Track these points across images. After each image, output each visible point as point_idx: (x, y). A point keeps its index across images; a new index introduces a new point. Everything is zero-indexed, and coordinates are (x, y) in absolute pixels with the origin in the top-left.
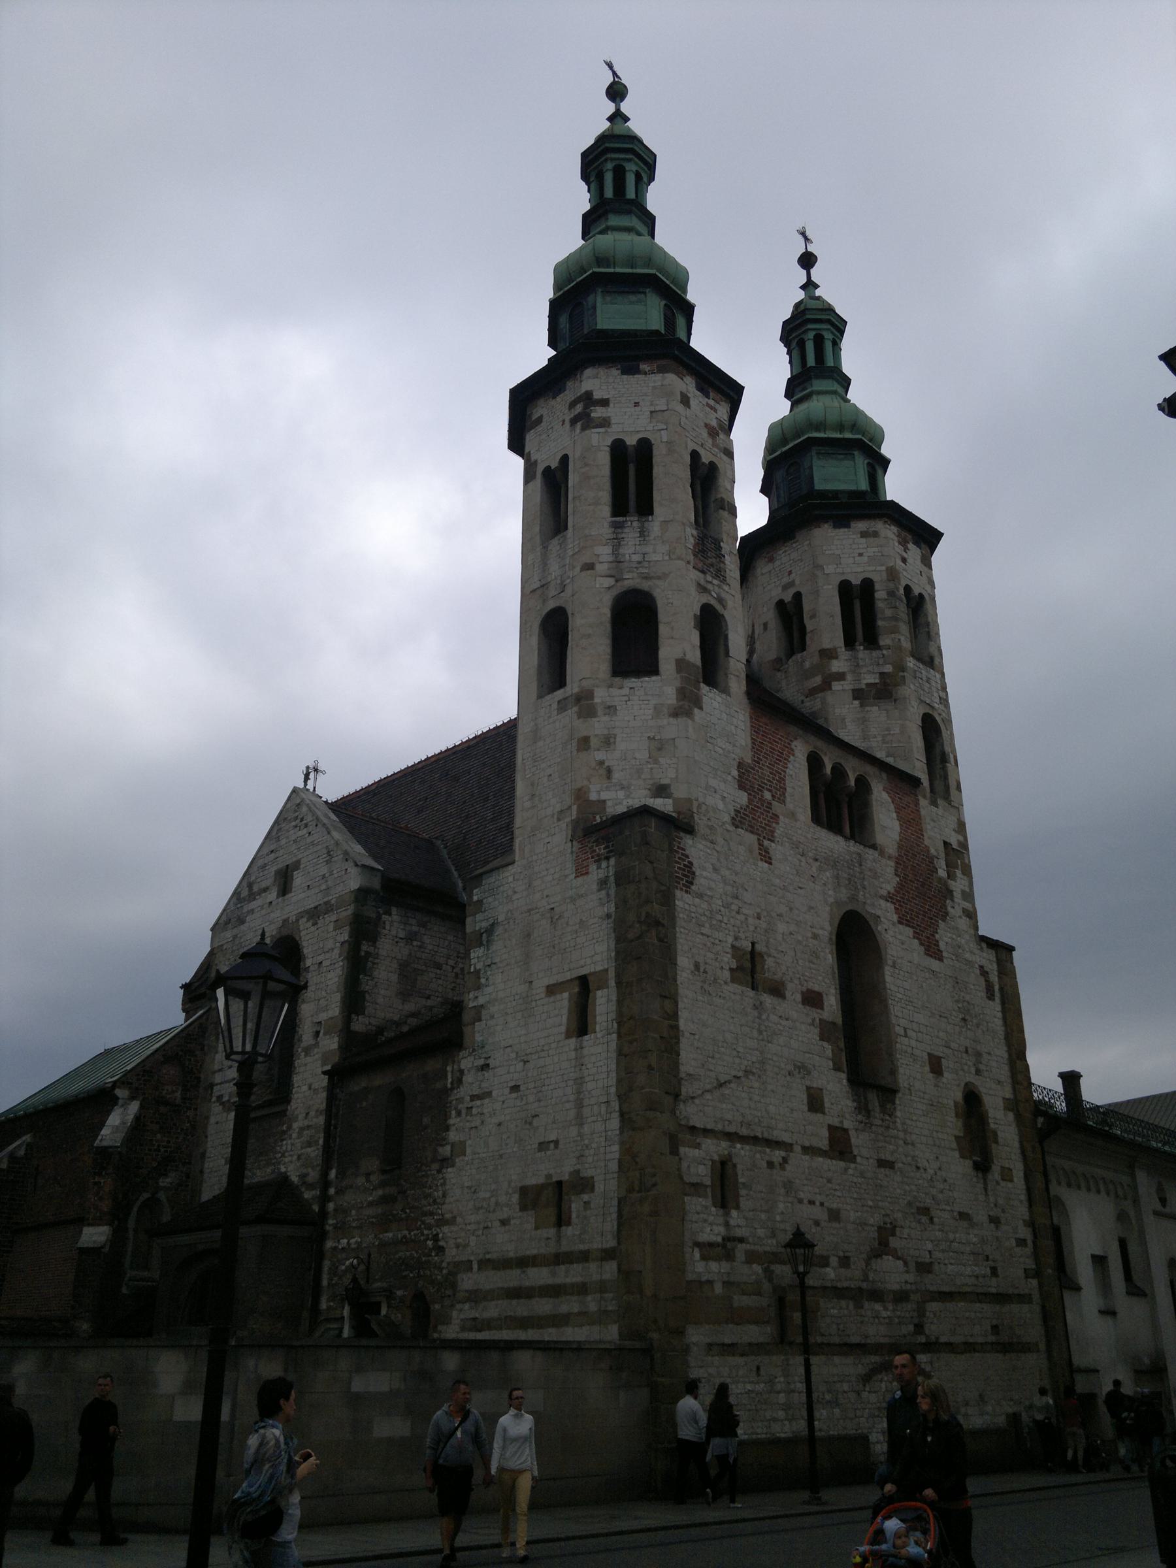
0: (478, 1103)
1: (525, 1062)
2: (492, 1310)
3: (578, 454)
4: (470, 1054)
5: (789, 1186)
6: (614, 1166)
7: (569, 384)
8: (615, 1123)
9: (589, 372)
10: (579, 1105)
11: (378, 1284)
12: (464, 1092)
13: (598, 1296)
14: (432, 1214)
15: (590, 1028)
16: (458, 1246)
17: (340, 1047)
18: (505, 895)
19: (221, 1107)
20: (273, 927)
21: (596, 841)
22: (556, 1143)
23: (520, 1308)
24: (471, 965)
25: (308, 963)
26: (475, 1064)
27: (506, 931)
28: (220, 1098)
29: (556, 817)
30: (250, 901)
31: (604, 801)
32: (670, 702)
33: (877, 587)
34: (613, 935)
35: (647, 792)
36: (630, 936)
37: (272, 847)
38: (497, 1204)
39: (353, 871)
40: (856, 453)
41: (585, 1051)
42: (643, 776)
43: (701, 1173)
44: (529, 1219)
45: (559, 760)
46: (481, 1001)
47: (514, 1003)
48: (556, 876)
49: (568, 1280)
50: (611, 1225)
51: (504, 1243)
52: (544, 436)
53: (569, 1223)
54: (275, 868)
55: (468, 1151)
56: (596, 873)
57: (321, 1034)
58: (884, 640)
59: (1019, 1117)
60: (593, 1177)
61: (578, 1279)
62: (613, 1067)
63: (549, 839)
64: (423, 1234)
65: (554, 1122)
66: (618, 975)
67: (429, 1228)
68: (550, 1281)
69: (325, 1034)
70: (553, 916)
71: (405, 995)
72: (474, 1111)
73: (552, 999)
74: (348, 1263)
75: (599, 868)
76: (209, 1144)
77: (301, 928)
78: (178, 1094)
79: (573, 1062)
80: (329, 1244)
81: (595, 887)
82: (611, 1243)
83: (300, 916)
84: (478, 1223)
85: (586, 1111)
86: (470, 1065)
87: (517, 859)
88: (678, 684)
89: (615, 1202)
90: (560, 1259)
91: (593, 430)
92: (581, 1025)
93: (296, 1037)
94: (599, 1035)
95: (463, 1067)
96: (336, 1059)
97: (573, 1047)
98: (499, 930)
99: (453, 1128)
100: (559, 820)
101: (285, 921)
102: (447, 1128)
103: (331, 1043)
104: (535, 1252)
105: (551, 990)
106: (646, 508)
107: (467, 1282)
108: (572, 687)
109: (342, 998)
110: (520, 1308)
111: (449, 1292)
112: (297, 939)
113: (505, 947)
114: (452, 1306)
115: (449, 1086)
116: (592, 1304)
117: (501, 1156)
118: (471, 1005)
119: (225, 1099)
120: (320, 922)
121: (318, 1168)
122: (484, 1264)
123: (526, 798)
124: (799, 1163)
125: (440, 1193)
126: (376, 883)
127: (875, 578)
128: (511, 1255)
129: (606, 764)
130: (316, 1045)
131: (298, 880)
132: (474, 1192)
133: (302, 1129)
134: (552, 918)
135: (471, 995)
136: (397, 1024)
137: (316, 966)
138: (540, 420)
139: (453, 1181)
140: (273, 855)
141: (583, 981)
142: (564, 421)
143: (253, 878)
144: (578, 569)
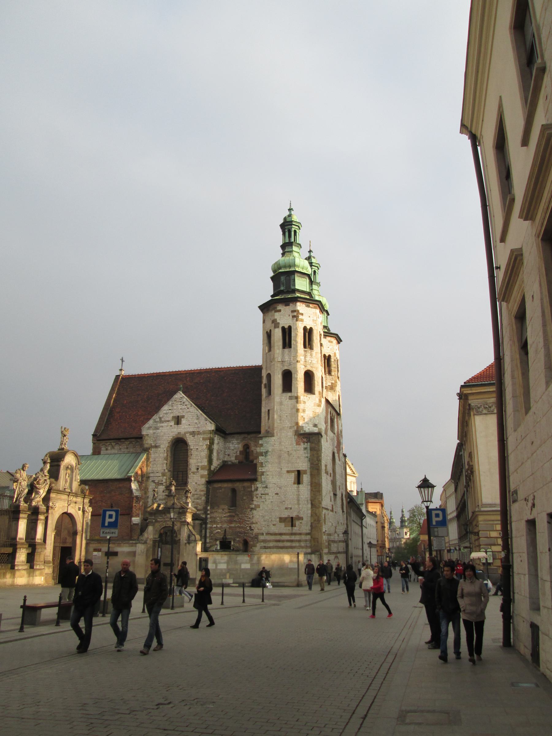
0: (264, 496)
1: (280, 488)
2: (271, 544)
3: (295, 328)
4: (260, 483)
5: (329, 518)
6: (309, 515)
7: (291, 304)
8: (310, 506)
9: (298, 304)
10: (298, 500)
11: (229, 537)
12: (258, 492)
13: (305, 543)
14: (249, 521)
15: (301, 482)
16: (258, 529)
17: (208, 474)
18: (271, 444)
19: (154, 484)
20: (173, 433)
21: (304, 438)
22: (291, 508)
23: (280, 544)
24: (259, 461)
25: (192, 448)
26: (263, 486)
27: (272, 454)
28: (153, 481)
29: (289, 428)
30: (160, 423)
31: (303, 427)
32: (317, 402)
33: (332, 358)
34: (309, 462)
35: (312, 426)
36: (315, 463)
37: (170, 408)
38: (271, 520)
39: (209, 424)
40: (325, 313)
41: (300, 488)
42: (312, 421)
43: (323, 517)
44: (283, 525)
45: (289, 412)
46: (263, 470)
47: (275, 473)
48: (289, 443)
49: (295, 539)
50: (309, 528)
51: (273, 529)
52: (282, 316)
53: (295, 526)
54: (172, 415)
55: (261, 507)
56: (302, 446)
57: (200, 469)
58: (333, 374)
59: (346, 499)
60: (303, 517)
61: (298, 539)
62: (309, 493)
63: (287, 433)
64: (245, 526)
65: (290, 503)
66: (311, 472)
67: (248, 524)
68: (289, 539)
69: (201, 469)
70: (289, 453)
71: (218, 459)
72: (263, 498)
73: (289, 474)
74: (217, 531)
75: (304, 444)
76: (150, 494)
77: (187, 436)
78: (140, 479)
79: (296, 490)
80: (209, 526)
81: (303, 449)
82: (308, 532)
83: (185, 433)
84: (265, 524)
85: (300, 502)
86: (260, 486)
87: (275, 435)
88: (319, 398)
89: (310, 523)
90: (292, 534)
91: (300, 322)
92: (298, 481)
93: (188, 468)
94: (304, 485)
95: (258, 486)
96: (207, 477)
97: (296, 486)
98: (269, 453)
99: (254, 501)
100: (290, 429)
101: (179, 433)
102: (253, 501)
103: (206, 473)
104: (285, 532)
105: (288, 472)
106: (311, 348)
107: (261, 538)
108: (293, 394)
109: (208, 460)
110: (280, 544)
111: (255, 540)
112: (186, 439)
113: (272, 458)
114: (257, 543)
115: (253, 490)
116: (303, 544)
117: (273, 509)
118: (260, 471)
119: (156, 481)
120: (196, 436)
121: (202, 506)
122: (268, 534)
123: (278, 420)
124: (331, 513)
125: (251, 516)
126: (215, 429)
127: (332, 355)
128: (277, 532)
129: (304, 417)
130: (199, 472)
131: (184, 421)
132: (264, 517)
133: (193, 495)
134: (288, 454)
135: (260, 468)
136: (217, 467)
137: (195, 449)
138: (280, 311)
139: (256, 514)
140: (170, 411)
141: (299, 472)
142: (289, 315)
143: (161, 416)
144: (296, 361)
